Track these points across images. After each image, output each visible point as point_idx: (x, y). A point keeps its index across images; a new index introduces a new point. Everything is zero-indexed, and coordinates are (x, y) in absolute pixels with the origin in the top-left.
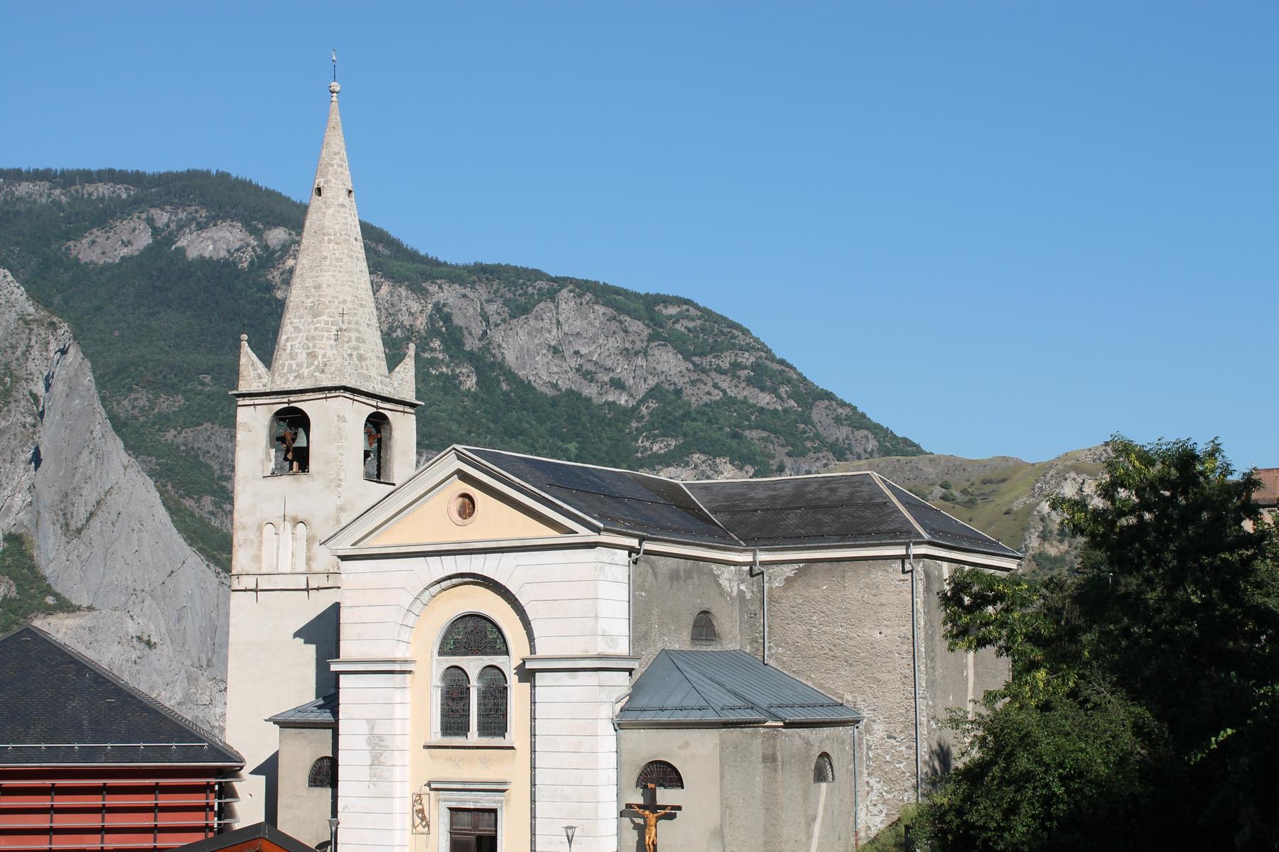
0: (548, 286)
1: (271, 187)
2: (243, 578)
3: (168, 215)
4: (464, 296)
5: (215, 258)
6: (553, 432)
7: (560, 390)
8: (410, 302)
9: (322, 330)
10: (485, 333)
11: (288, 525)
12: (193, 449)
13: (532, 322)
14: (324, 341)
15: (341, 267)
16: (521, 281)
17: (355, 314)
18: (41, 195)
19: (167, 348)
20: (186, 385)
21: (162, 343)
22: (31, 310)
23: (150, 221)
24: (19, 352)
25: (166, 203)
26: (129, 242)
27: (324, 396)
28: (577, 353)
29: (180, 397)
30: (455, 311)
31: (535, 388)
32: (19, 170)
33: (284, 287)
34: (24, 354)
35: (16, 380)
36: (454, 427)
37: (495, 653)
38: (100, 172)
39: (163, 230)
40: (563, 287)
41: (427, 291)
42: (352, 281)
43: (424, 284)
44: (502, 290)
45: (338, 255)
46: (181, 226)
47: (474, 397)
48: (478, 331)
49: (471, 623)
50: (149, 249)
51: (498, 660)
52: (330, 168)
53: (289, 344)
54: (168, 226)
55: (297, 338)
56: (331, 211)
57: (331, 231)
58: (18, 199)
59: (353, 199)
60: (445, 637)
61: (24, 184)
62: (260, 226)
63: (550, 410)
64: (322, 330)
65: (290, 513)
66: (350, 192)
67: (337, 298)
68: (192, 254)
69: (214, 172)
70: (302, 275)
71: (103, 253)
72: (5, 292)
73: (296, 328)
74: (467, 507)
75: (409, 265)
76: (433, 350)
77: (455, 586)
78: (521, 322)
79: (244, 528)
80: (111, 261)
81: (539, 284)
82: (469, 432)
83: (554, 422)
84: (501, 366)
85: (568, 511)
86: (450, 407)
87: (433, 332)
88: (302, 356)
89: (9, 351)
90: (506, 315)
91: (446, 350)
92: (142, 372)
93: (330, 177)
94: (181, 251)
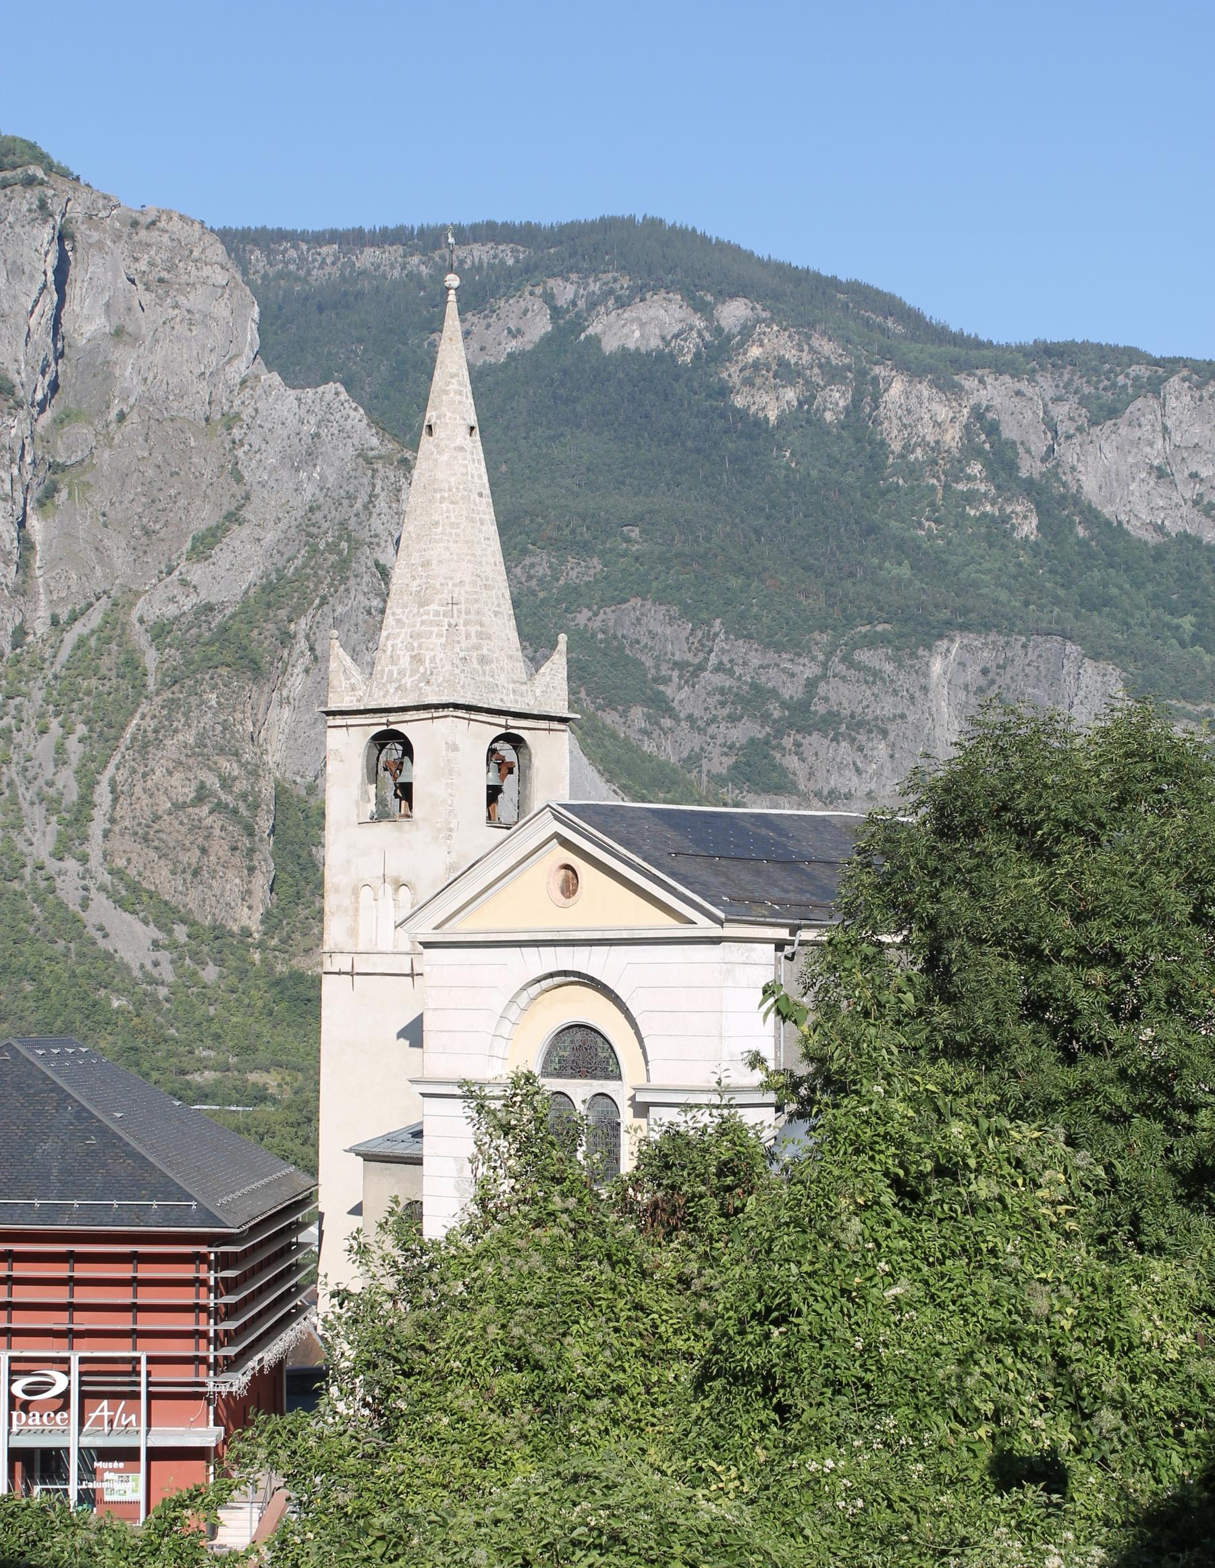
0: (1149, 373)
1: (725, 238)
2: (337, 958)
3: (574, 287)
4: (1018, 393)
5: (643, 350)
6: (1156, 600)
7: (1168, 535)
8: (935, 407)
9: (431, 623)
10: (1051, 450)
11: (389, 888)
12: (615, 637)
13: (1124, 430)
14: (433, 639)
15: (457, 535)
16: (1107, 366)
17: (477, 601)
18: (392, 267)
19: (576, 488)
20: (603, 543)
21: (568, 481)
22: (375, 441)
23: (549, 298)
24: (359, 505)
25: (570, 270)
26: (519, 331)
27: (429, 715)
28: (1194, 476)
29: (595, 560)
30: (1005, 417)
31: (1128, 533)
32: (361, 230)
33: (746, 389)
34: (366, 507)
35: (355, 545)
36: (1003, 596)
37: (607, 1078)
38: (474, 227)
39: (568, 311)
40: (1172, 373)
41: (961, 388)
42: (473, 555)
43: (956, 378)
44: (1077, 382)
45: (453, 519)
46: (593, 305)
47: (1035, 549)
48: (1039, 447)
49: (579, 1036)
50: (547, 340)
51: (608, 1086)
52: (444, 397)
53: (389, 643)
54: (574, 303)
55: (399, 634)
56: (445, 457)
57: (446, 486)
58: (360, 274)
59: (478, 438)
60: (549, 1053)
61: (368, 251)
62: (709, 298)
63: (1152, 565)
64: (431, 623)
65: (391, 873)
66: (472, 428)
67: (452, 578)
68: (610, 345)
69: (639, 218)
70: (407, 547)
71: (482, 349)
72: (338, 416)
73: (399, 621)
74: (570, 885)
75: (931, 348)
76: (970, 478)
77: (560, 986)
78: (1106, 431)
79: (337, 891)
80: (493, 360)
81: (1135, 370)
82: (1027, 604)
83: (1159, 584)
84: (1075, 500)
85: (683, 895)
86: (997, 565)
87: (971, 450)
88: (405, 661)
89: (345, 502)
90: (1083, 421)
91: (992, 477)
92: (540, 525)
93: (444, 409)
94: (595, 341)
